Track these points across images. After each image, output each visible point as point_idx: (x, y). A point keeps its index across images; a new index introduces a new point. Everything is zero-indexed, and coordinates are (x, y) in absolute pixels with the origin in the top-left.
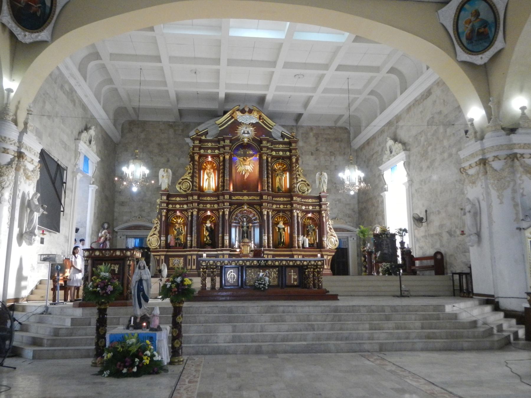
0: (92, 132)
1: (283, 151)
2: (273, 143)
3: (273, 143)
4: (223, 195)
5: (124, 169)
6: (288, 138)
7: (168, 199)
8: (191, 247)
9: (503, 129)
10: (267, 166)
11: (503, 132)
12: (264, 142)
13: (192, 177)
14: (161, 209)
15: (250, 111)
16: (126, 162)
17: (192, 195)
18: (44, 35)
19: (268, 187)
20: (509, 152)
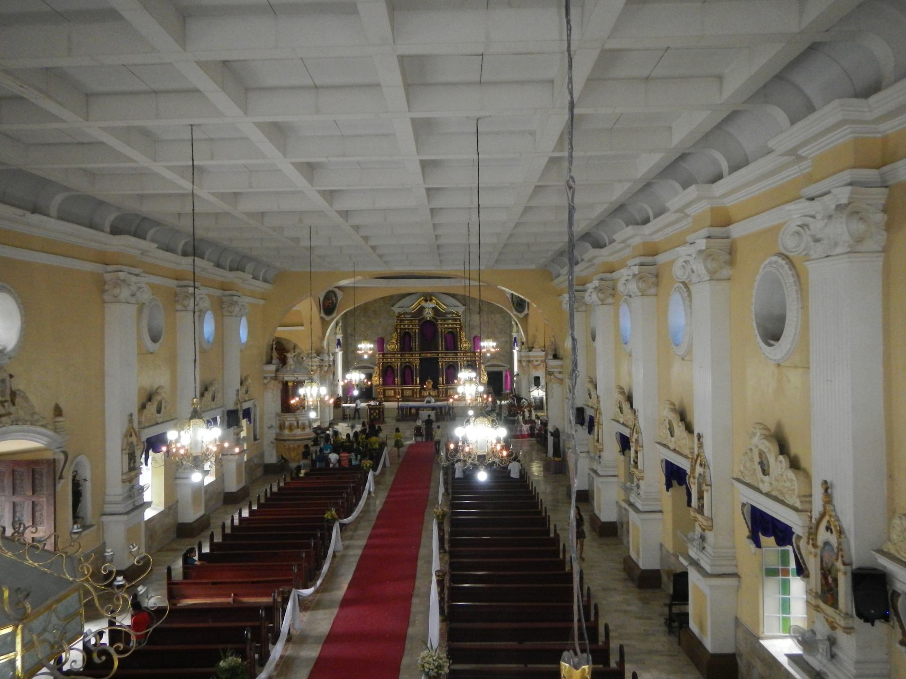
0: (340, 324)
1: (452, 324)
2: (445, 320)
3: (445, 320)
4: (415, 354)
5: (359, 346)
6: (455, 314)
7: (383, 356)
8: (398, 384)
9: (529, 348)
10: (442, 335)
11: (527, 350)
12: (439, 321)
13: (397, 341)
14: (379, 363)
15: (431, 300)
16: (361, 343)
17: (397, 354)
18: (334, 315)
19: (442, 347)
20: (527, 359)
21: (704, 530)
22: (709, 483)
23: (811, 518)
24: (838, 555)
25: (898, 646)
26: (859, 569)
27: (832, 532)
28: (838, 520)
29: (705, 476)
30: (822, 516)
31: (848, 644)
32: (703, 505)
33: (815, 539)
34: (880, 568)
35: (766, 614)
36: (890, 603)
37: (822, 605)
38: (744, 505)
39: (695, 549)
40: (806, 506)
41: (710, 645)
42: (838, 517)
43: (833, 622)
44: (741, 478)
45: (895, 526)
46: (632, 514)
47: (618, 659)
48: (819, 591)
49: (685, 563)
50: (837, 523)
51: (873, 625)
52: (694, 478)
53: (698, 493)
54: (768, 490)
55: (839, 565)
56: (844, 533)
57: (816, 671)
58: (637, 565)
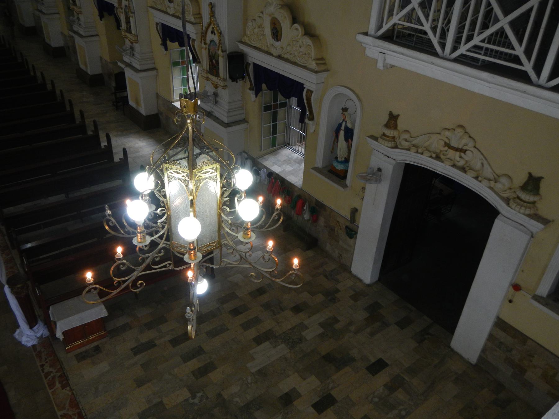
21: (132, 43)
22: (132, 11)
23: (203, 26)
24: (219, 46)
25: (248, 91)
26: (230, 53)
27: (215, 34)
28: (218, 26)
29: (130, 7)
30: (209, 25)
31: (224, 95)
32: (130, 27)
33: (205, 40)
34: (240, 51)
35: (174, 88)
36: (245, 69)
37: (210, 76)
38: (157, 24)
39: (128, 57)
40: (198, 21)
41: (143, 111)
42: (218, 25)
43: (216, 84)
44: (154, 6)
45: (249, 27)
46: (77, 39)
47: (93, 128)
48: (208, 69)
49: (122, 66)
50: (218, 28)
51: (237, 82)
52: (122, 9)
53: (126, 19)
54: (173, 13)
55: (220, 52)
56: (222, 34)
57: (208, 112)
58: (86, 73)
